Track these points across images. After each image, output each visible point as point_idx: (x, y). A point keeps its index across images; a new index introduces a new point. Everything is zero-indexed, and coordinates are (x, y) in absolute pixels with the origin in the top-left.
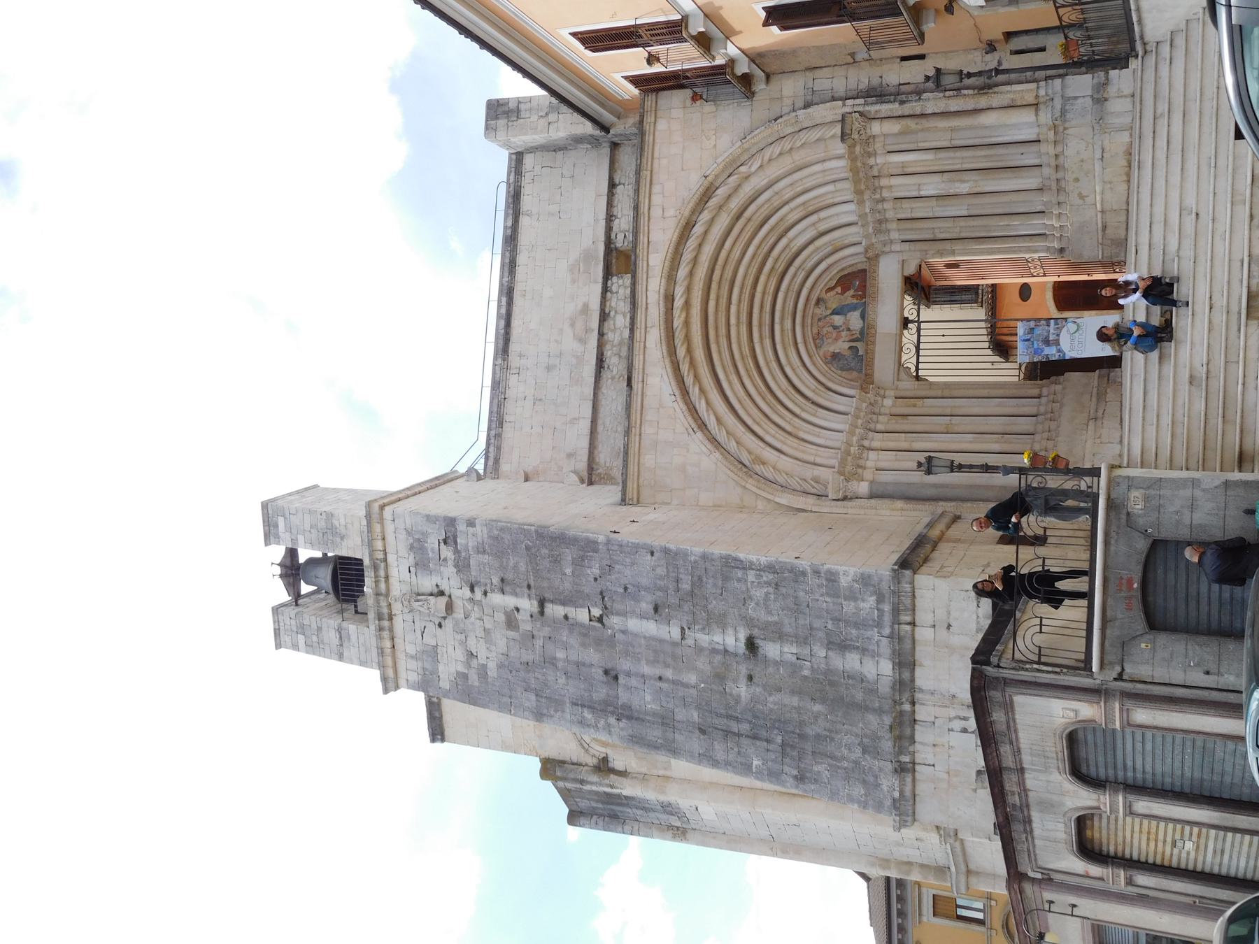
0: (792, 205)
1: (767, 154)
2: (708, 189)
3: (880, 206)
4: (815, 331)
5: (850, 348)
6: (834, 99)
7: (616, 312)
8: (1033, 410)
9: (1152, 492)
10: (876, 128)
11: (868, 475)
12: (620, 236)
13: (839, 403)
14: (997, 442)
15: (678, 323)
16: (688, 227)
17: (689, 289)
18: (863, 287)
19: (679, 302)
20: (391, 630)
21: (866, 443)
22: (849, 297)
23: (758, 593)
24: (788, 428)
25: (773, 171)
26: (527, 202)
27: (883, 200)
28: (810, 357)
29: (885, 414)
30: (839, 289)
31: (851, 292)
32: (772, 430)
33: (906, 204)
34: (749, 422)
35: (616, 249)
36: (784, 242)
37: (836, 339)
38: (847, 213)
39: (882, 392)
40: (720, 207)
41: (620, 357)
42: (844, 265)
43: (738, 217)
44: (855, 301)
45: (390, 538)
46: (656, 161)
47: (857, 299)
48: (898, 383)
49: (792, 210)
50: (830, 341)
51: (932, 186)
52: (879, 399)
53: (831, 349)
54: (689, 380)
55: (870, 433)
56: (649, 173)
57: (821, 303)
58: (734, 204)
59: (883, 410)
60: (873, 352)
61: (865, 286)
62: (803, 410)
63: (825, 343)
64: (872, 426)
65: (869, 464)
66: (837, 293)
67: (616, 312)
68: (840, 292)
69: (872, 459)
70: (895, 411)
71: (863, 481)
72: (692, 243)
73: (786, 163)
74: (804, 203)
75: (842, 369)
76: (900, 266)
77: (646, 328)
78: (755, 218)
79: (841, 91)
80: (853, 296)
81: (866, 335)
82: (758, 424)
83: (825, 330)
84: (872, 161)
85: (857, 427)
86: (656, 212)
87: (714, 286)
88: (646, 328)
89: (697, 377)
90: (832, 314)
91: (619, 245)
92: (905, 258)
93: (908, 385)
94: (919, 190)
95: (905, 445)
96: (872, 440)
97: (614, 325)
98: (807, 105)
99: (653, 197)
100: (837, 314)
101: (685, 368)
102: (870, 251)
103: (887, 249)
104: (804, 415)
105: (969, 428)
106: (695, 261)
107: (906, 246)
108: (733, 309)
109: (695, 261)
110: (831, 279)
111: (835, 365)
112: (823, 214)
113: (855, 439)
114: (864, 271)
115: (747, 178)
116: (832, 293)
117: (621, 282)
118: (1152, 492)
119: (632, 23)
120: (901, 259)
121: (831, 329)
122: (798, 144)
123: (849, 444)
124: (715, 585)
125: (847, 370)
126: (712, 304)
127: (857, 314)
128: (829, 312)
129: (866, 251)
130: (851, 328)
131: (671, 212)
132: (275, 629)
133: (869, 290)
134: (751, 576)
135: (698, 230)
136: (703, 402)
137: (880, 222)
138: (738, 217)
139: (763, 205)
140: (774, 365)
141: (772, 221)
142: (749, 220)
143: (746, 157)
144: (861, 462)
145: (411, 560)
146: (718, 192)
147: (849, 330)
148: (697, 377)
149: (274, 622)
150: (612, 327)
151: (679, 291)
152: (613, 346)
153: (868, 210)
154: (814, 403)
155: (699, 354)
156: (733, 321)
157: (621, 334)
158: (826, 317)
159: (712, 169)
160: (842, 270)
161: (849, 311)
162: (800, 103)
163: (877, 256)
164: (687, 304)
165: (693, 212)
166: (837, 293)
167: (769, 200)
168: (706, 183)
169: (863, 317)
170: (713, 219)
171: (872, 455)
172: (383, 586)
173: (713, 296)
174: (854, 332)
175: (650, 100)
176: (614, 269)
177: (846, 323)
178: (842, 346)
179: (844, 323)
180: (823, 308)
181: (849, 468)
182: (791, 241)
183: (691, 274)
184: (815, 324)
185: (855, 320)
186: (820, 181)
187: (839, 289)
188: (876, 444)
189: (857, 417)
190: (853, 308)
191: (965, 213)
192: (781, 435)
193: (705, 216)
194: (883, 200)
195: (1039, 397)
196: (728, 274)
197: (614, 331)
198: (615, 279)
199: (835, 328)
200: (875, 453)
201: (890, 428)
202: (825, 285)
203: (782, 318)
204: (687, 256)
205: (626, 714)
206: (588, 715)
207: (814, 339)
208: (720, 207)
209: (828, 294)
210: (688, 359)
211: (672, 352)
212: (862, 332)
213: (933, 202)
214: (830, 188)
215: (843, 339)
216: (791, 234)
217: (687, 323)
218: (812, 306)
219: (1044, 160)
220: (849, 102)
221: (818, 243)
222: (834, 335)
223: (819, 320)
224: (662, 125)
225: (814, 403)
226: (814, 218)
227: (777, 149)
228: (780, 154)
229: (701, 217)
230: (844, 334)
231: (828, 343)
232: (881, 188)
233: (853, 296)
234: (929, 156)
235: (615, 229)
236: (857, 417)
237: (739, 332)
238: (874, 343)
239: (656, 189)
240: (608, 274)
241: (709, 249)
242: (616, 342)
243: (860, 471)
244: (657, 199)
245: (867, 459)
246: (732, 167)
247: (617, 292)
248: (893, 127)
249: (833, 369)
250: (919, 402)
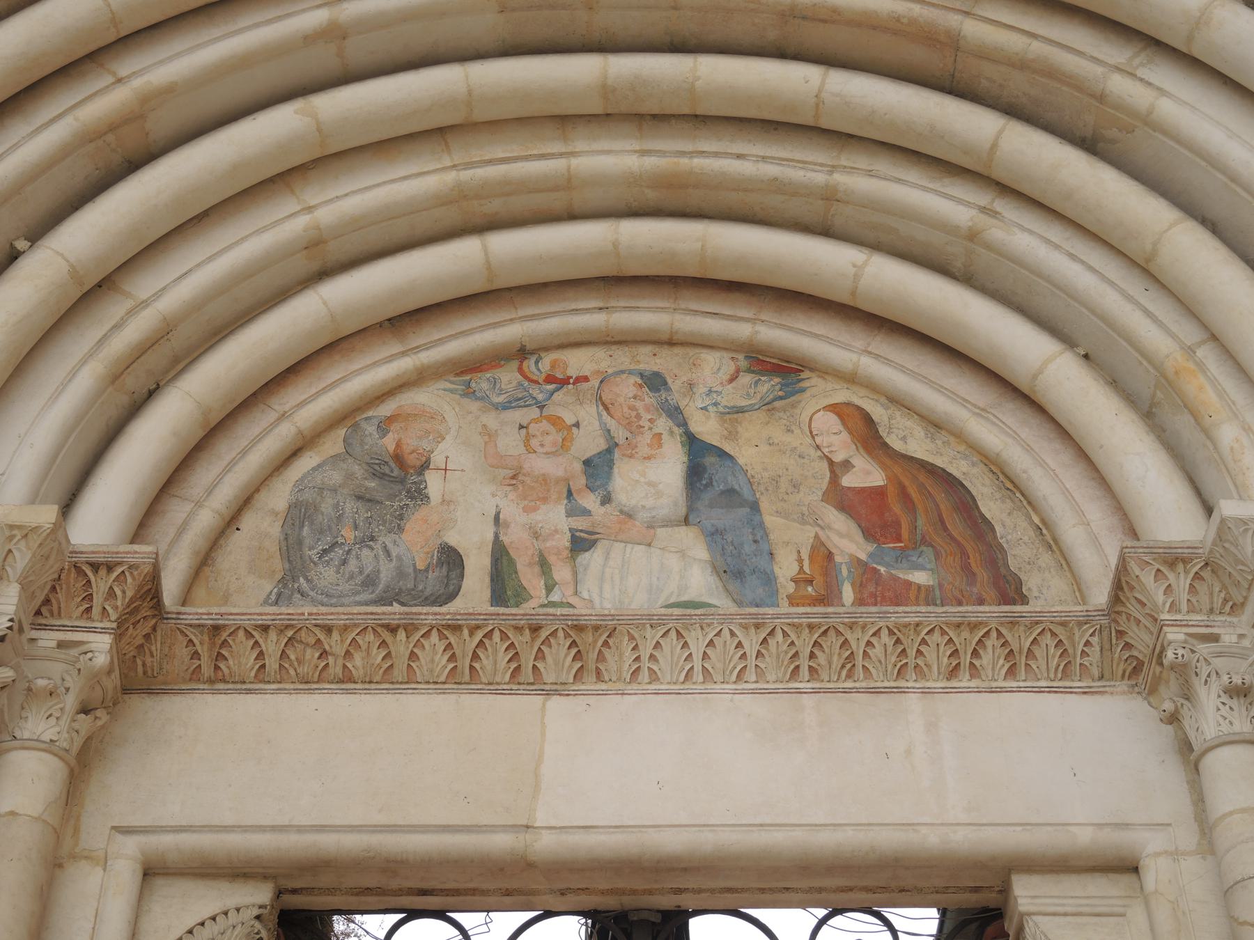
4: (578, 362)
5: (451, 559)
42: (1042, 485)
44: (785, 569)
47: (801, 580)
48: (125, 873)
50: (510, 443)
53: (447, 451)
57: (769, 385)
63: (491, 420)
66: (837, 469)
68: (847, 481)
75: (299, 514)
76: (1083, 838)
80: (823, 556)
83: (588, 414)
90: (695, 447)
92: (1155, 873)
100: (695, 475)
102: (1181, 582)
110: (935, 424)
111: (334, 477)
116: (839, 443)
120: (1150, 845)
121: (589, 443)
125: (291, 547)
128: (707, 428)
130: (592, 559)
147: (581, 544)
158: (675, 414)
161: (714, 536)
166: (837, 469)
174: (561, 573)
179: (629, 515)
180: (732, 396)
184: (622, 358)
202: (895, 400)
207: (522, 353)
209: (830, 421)
215: (511, 510)
218: (743, 331)
222: (541, 465)
223: (655, 382)
230: (555, 518)
231: (489, 435)
233: (823, 556)
249: (307, 462)
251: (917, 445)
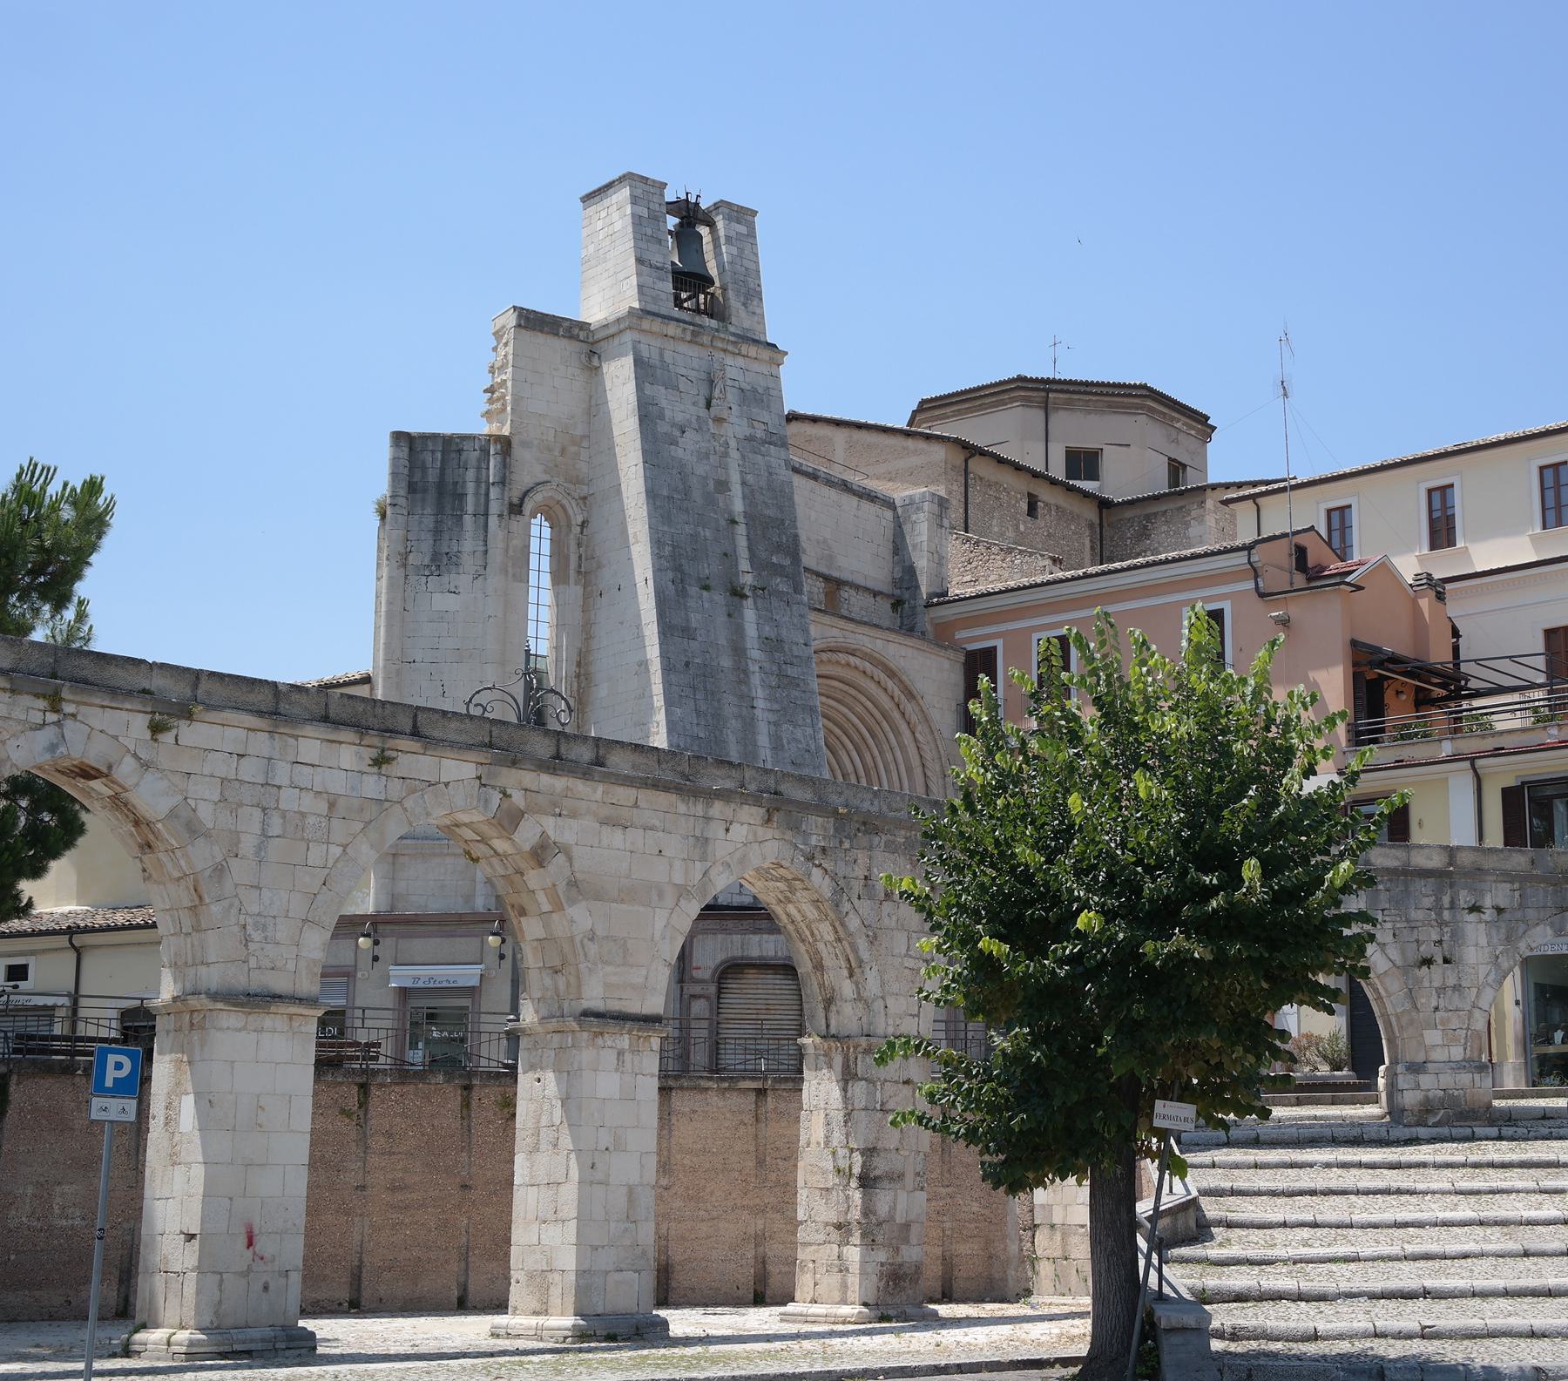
0: (879, 759)
16: (892, 674)
20: (683, 340)
23: (799, 734)
26: (866, 506)
45: (756, 367)
46: (928, 655)
49: (873, 758)
87: (846, 688)
124: (796, 698)
132: (648, 179)
134: (809, 731)
141: (870, 741)
145: (744, 386)
149: (654, 181)
165: (901, 681)
172: (720, 345)
175: (962, 658)
196: (848, 700)
205: (682, 593)
206: (668, 549)
216: (854, 754)
224: (946, 664)
241: (872, 688)
244: (910, 652)
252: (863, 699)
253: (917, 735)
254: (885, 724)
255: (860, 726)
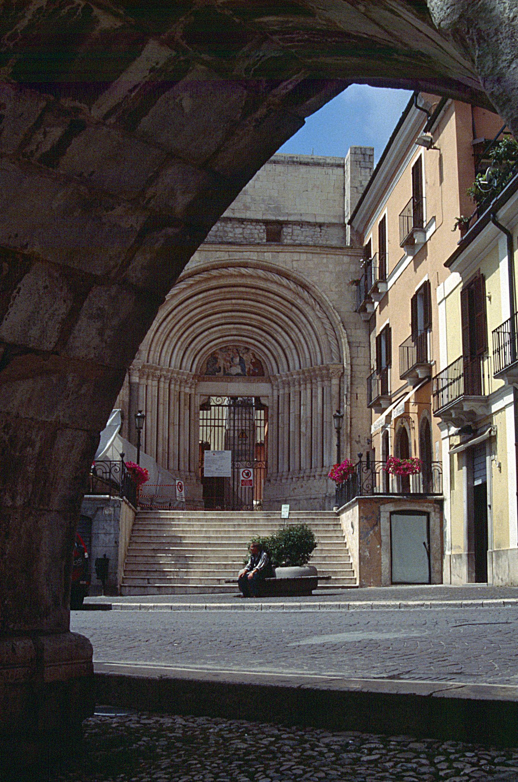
0: (299, 334)
1: (325, 321)
2: (308, 287)
3: (296, 383)
4: (230, 347)
6: (352, 358)
7: (244, 228)
8: (182, 468)
9: (113, 517)
10: (335, 381)
11: (143, 381)
12: (290, 230)
13: (187, 363)
14: (163, 450)
15: (231, 270)
17: (251, 276)
18: (254, 374)
19: (243, 270)
21: (162, 379)
22: (248, 366)
24: (171, 335)
25: (316, 324)
27: (300, 385)
28: (215, 345)
29: (180, 389)
30: (254, 361)
31: (252, 368)
32: (170, 326)
33: (297, 397)
34: (174, 313)
35: (282, 228)
36: (280, 330)
37: (225, 360)
38: (294, 363)
39: (193, 387)
40: (298, 294)
41: (217, 231)
43: (293, 304)
44: (247, 370)
46: (325, 256)
50: (225, 356)
51: (305, 412)
52: (190, 385)
54: (197, 278)
55: (168, 381)
56: (319, 252)
58: (299, 302)
59: (183, 388)
60: (218, 381)
61: (254, 376)
62: (182, 343)
64: (173, 382)
65: (150, 381)
67: (244, 228)
69: (153, 383)
70: (182, 394)
71: (140, 378)
72: (276, 278)
73: (320, 332)
74: (300, 341)
77: (229, 251)
78: (292, 313)
79: (356, 362)
80: (249, 368)
81: (228, 377)
82: (173, 318)
83: (231, 353)
84: (319, 379)
85: (172, 373)
86: (296, 257)
87: (253, 291)
88: (229, 251)
89: (199, 282)
90: (240, 357)
91: (284, 229)
93: (198, 401)
94: (304, 405)
95: (161, 401)
96: (164, 382)
97: (237, 227)
98: (349, 343)
99: (305, 255)
100: (240, 360)
101: (205, 275)
103: (274, 387)
104: (179, 343)
105: (171, 434)
106: (266, 280)
107: (276, 398)
108: (241, 301)
109: (266, 280)
112: (294, 351)
113: (165, 373)
114: (263, 375)
115: (313, 309)
117: (262, 231)
118: (113, 517)
119: (387, 252)
121: (231, 356)
122: (330, 339)
123: (161, 370)
126: (243, 289)
127: (240, 371)
128: (241, 355)
129: (274, 376)
131: (295, 264)
133: (253, 378)
135: (285, 281)
136: (185, 286)
137: (289, 384)
138: (293, 304)
139: (300, 319)
140: (209, 325)
141: (290, 323)
142: (291, 310)
143: (325, 309)
144: (151, 377)
146: (306, 293)
147: (231, 367)
148: (199, 282)
150: (235, 226)
151: (250, 271)
152: (224, 227)
153: (294, 377)
154: (187, 349)
155: (214, 283)
156: (234, 301)
157: (230, 232)
159: (318, 290)
160: (265, 363)
162: (352, 339)
163: (271, 382)
164: (243, 276)
167: (302, 322)
168: (310, 286)
169: (238, 375)
170: (290, 289)
171: (155, 383)
173: (248, 290)
176: (269, 227)
177: (235, 365)
178: (221, 363)
180: (243, 352)
181: (147, 370)
182: (280, 334)
183: (260, 278)
185: (237, 370)
186: (311, 351)
187: (254, 361)
188: (162, 385)
189: (178, 373)
190: (243, 370)
191: (291, 430)
192: (167, 331)
193: (292, 286)
194: (300, 385)
195: (190, 471)
197: (232, 227)
198: (264, 227)
199: (232, 359)
200: (157, 384)
201: (172, 391)
203: (236, 329)
204: (270, 275)
207: (226, 347)
208: (298, 294)
210: (209, 276)
211: (215, 268)
212: (229, 374)
213: (297, 413)
214: (308, 356)
216: (283, 333)
217: (231, 275)
219: (313, 470)
220: (349, 367)
221: (279, 348)
224: (346, 259)
225: (187, 349)
226: (292, 346)
227: (328, 326)
228: (325, 329)
229: (292, 283)
232: (306, 384)
233: (249, 368)
234: (320, 411)
235: (295, 227)
236: (178, 373)
237: (228, 305)
238: (222, 381)
239: (310, 256)
240: (266, 223)
242: (225, 229)
243: (145, 377)
244: (304, 257)
245: (152, 380)
246: (319, 302)
247: (256, 229)
248: (335, 389)
250: (187, 407)
251: (258, 358)
252: (271, 296)
253: (317, 313)
254: (294, 309)
255: (279, 314)
